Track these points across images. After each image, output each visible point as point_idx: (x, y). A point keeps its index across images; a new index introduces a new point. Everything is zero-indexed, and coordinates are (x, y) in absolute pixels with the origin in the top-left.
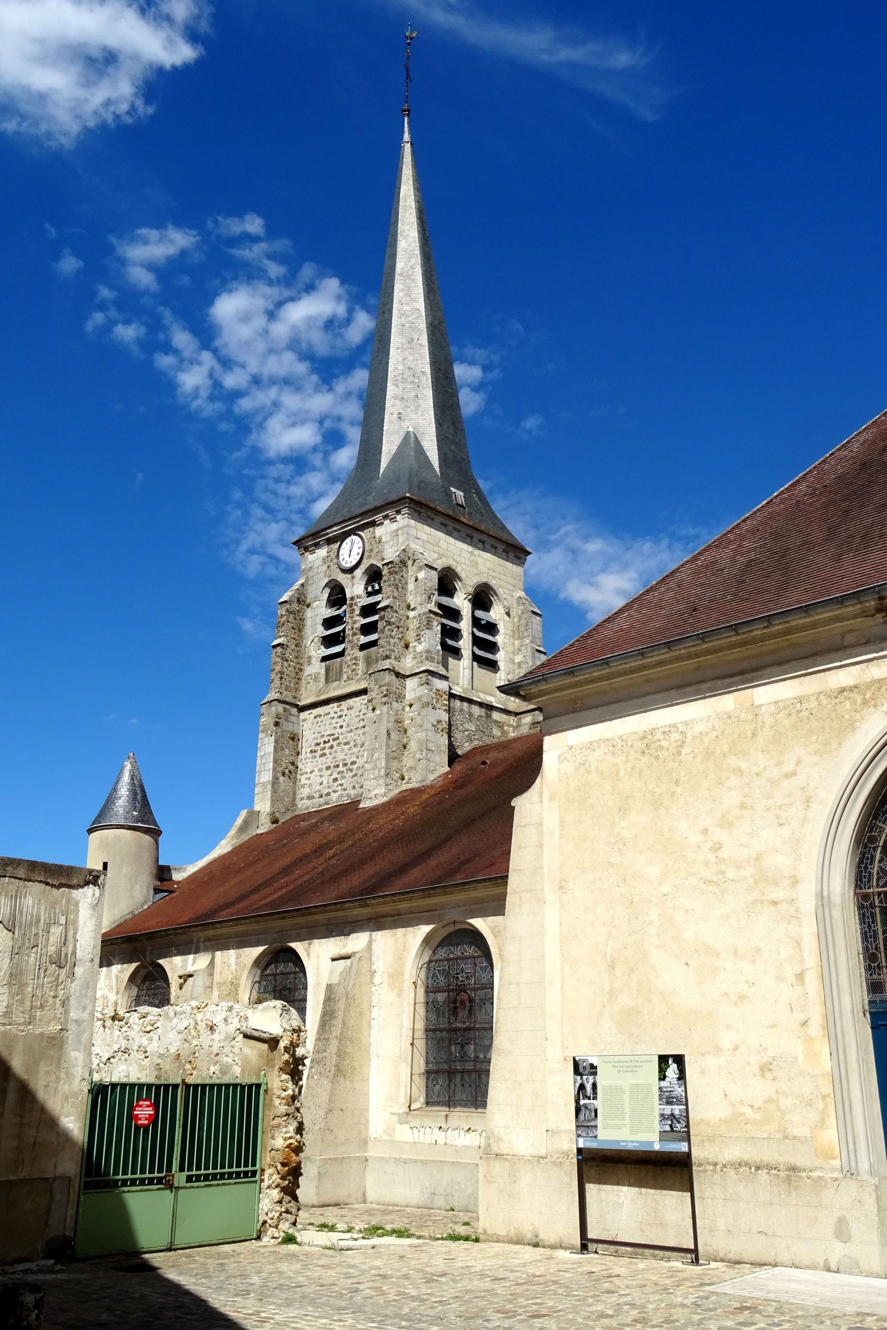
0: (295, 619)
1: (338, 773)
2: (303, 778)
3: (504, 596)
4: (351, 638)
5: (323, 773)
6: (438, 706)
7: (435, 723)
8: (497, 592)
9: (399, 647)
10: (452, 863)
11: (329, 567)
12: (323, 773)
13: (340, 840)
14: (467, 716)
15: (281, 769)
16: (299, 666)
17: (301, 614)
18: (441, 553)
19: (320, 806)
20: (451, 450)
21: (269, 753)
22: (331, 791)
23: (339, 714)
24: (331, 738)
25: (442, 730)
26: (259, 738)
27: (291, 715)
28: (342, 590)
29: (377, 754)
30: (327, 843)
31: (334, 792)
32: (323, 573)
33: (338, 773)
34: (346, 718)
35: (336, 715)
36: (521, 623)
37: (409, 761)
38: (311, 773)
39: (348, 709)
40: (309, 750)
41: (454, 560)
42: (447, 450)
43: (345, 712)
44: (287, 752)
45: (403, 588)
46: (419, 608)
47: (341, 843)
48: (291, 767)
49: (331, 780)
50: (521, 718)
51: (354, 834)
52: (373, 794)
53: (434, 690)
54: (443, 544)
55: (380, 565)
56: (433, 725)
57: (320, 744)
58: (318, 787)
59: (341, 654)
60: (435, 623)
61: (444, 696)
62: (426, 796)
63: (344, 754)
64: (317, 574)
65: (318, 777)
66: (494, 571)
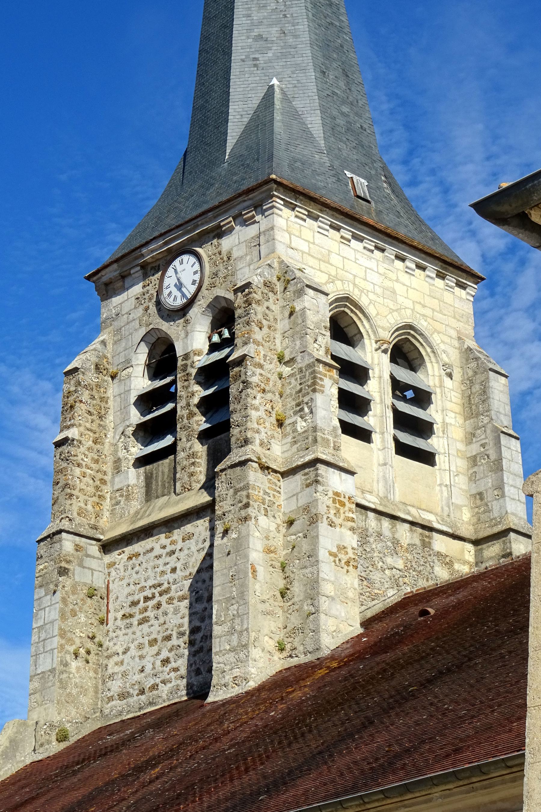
0: (93, 398)
1: (171, 650)
2: (111, 663)
3: (442, 346)
4: (185, 421)
5: (144, 652)
6: (338, 521)
7: (335, 550)
8: (431, 339)
9: (267, 424)
10: (377, 759)
11: (146, 309)
12: (144, 652)
13: (171, 753)
14: (389, 544)
15: (72, 649)
16: (100, 476)
17: (102, 390)
18: (333, 273)
19: (140, 709)
20: (343, 114)
21: (52, 622)
22: (158, 681)
23: (169, 549)
24: (156, 591)
25: (348, 563)
26: (36, 597)
27: (88, 556)
28: (171, 348)
29: (235, 607)
30: (147, 762)
31: (164, 682)
32: (137, 322)
33: (171, 650)
34: (182, 555)
35: (164, 552)
36: (474, 390)
37: (292, 618)
38: (124, 653)
39: (184, 540)
40: (119, 615)
41: (355, 285)
42: (335, 113)
43: (180, 545)
44: (83, 619)
45: (270, 327)
46: (299, 359)
47: (171, 757)
48: (90, 645)
49: (158, 663)
50: (481, 550)
51: (197, 741)
52: (228, 678)
53: (330, 494)
54: (335, 259)
55: (230, 296)
56: (331, 554)
57: (138, 602)
58: (137, 677)
59: (171, 450)
60: (327, 382)
61: (347, 503)
62: (323, 672)
63: (179, 615)
64: (128, 323)
65: (137, 659)
66: (424, 306)
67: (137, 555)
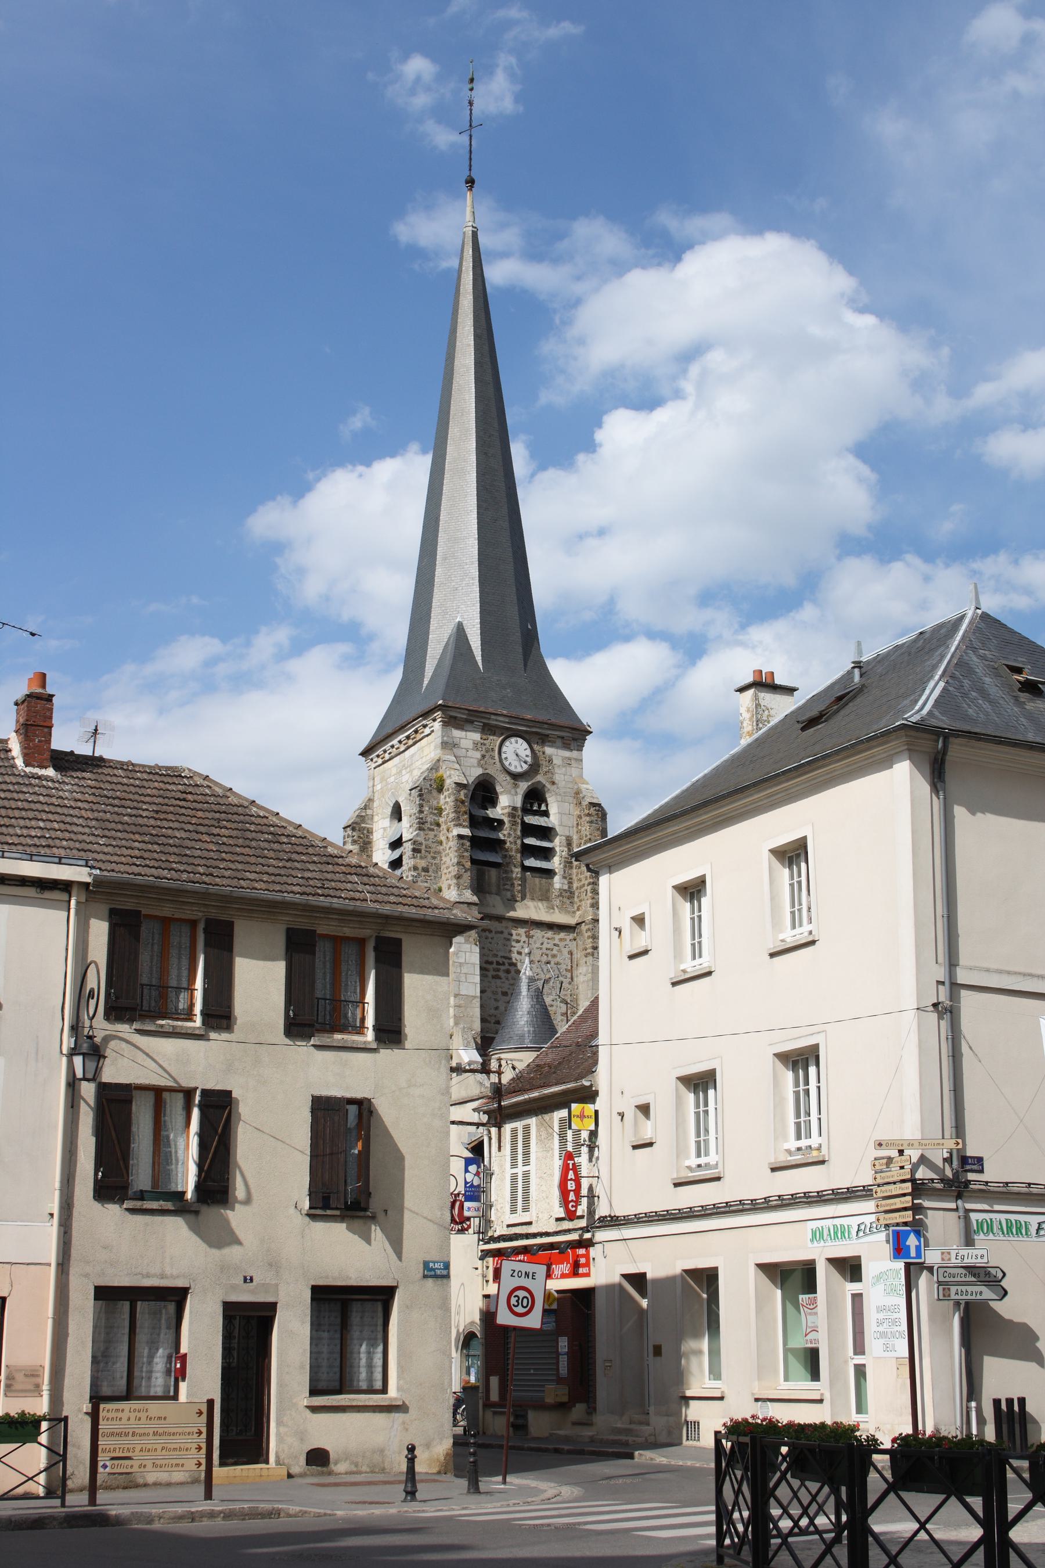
24: (506, 961)
58: (493, 1011)
67: (490, 931)
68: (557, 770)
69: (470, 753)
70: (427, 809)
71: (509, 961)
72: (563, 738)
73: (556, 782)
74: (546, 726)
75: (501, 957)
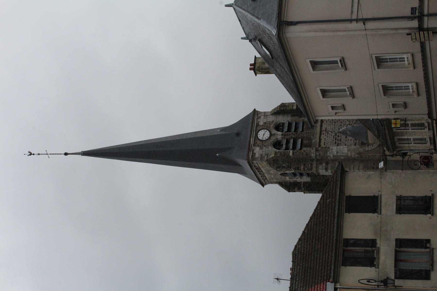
24: (335, 137)
58: (352, 141)
67: (325, 143)
68: (268, 120)
69: (264, 151)
70: (284, 165)
71: (335, 135)
72: (257, 119)
73: (272, 120)
74: (253, 125)
75: (333, 139)
